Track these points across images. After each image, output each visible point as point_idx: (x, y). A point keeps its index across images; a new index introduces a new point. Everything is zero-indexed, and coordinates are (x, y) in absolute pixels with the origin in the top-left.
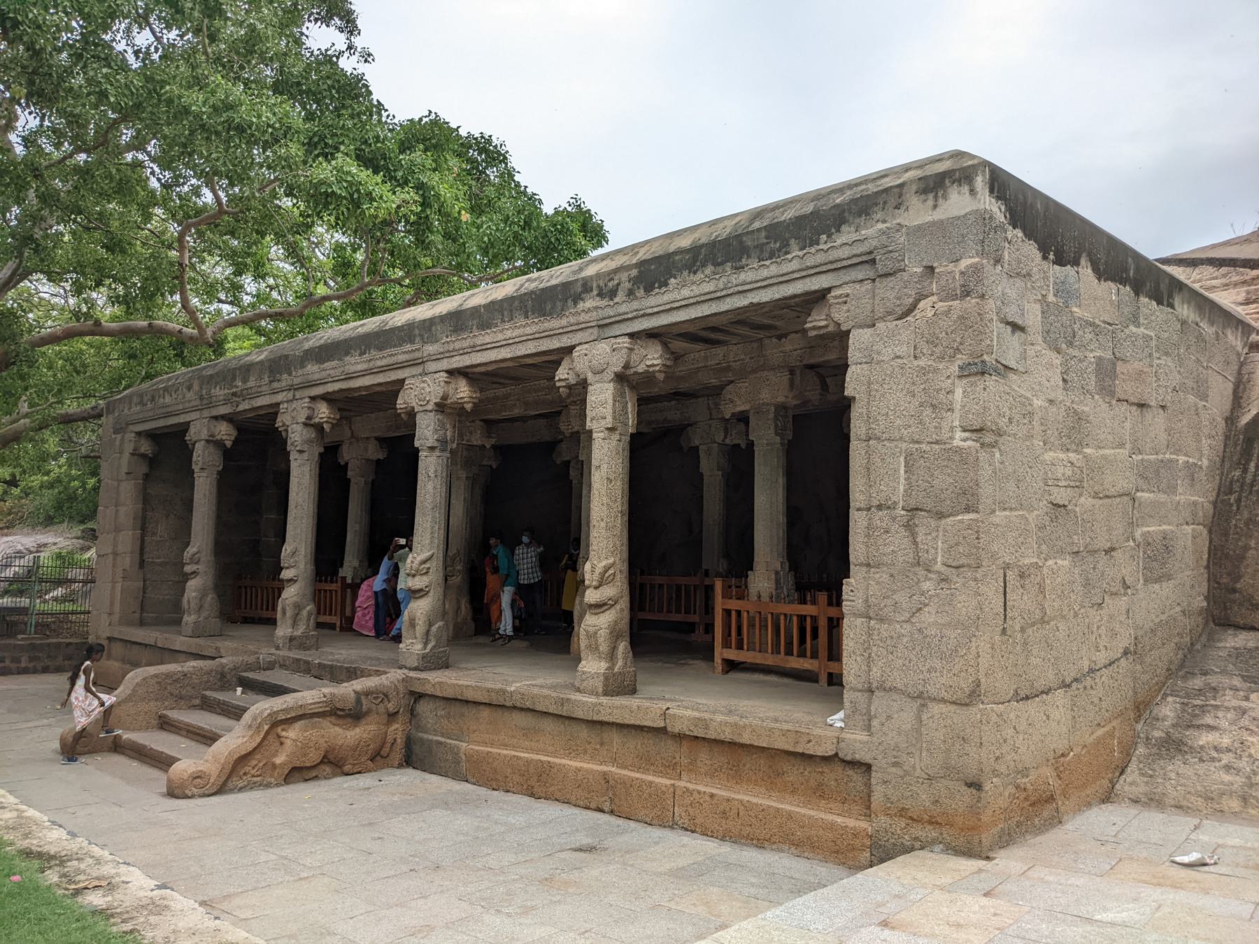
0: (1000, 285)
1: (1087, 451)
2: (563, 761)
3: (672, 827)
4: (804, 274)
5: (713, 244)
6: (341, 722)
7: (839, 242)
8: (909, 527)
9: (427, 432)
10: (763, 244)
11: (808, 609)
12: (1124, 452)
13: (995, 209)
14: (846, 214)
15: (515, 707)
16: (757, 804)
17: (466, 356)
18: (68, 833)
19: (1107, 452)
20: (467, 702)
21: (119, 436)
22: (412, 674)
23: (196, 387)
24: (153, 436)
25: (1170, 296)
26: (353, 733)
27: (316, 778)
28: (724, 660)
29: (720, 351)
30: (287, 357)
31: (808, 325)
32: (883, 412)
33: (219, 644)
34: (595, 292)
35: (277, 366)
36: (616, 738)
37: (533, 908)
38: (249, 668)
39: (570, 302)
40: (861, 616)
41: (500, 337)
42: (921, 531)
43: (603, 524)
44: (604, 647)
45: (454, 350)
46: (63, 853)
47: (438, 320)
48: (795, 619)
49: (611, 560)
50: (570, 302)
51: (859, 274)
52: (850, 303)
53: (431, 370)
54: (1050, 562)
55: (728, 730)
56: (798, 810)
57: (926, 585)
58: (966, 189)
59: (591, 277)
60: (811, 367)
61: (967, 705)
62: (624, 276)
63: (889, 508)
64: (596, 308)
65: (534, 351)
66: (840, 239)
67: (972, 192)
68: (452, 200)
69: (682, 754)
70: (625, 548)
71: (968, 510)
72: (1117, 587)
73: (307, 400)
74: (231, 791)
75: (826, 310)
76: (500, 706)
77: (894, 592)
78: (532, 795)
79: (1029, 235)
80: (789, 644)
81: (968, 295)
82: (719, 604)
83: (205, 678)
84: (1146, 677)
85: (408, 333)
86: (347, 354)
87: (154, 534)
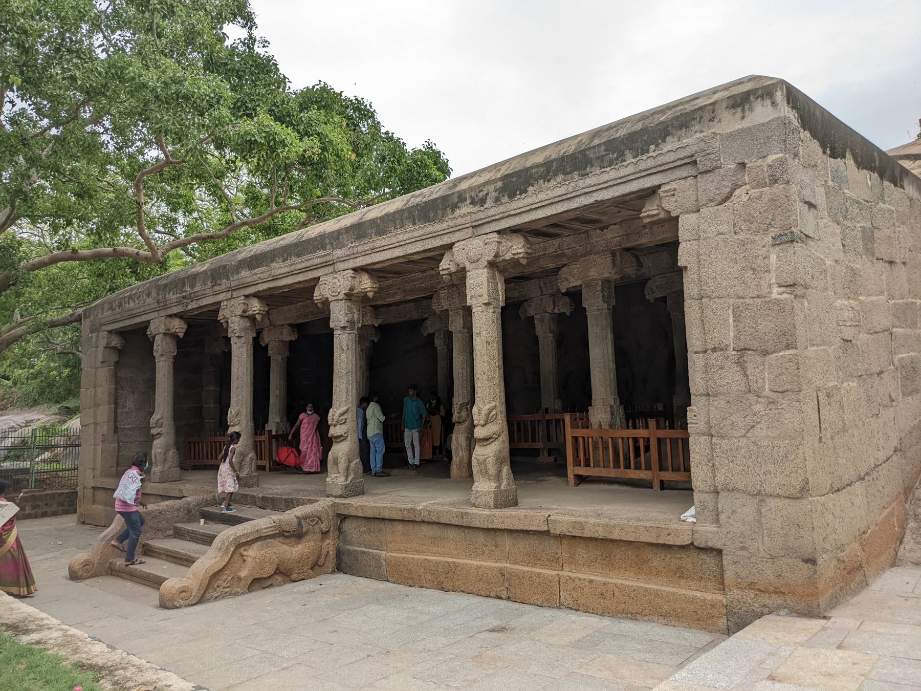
0: (798, 174)
1: (861, 298)
2: (465, 561)
3: (559, 608)
4: (638, 175)
5: (562, 159)
6: (287, 541)
7: (665, 150)
8: (740, 363)
9: (339, 315)
10: (604, 156)
11: (641, 433)
12: (883, 298)
13: (792, 117)
14: (670, 129)
15: (423, 522)
16: (629, 586)
18: (108, 646)
19: (873, 298)
20: (384, 519)
21: (95, 335)
22: (338, 501)
23: (154, 294)
24: (121, 333)
25: (902, 180)
26: (297, 549)
27: (271, 586)
28: (575, 475)
29: (556, 242)
30: (225, 267)
31: (643, 215)
32: (712, 276)
33: (181, 487)
34: (469, 201)
35: (217, 274)
36: (507, 542)
37: (475, 681)
38: (208, 503)
39: (449, 211)
40: (703, 435)
41: (394, 240)
42: (750, 366)
43: (485, 377)
44: (492, 471)
45: (358, 253)
46: (110, 664)
47: (343, 231)
48: (631, 440)
49: (493, 404)
50: (449, 211)
51: (683, 172)
52: (678, 194)
54: (845, 384)
55: (601, 530)
56: (663, 588)
57: (757, 408)
58: (768, 102)
59: (465, 190)
60: (628, 250)
61: (798, 498)
62: (491, 188)
63: (722, 350)
64: (470, 213)
65: (422, 249)
66: (666, 148)
67: (774, 104)
68: (333, 146)
69: (563, 550)
70: (503, 394)
71: (788, 347)
72: (886, 401)
73: (243, 298)
74: (208, 600)
75: (657, 202)
76: (411, 521)
77: (731, 414)
78: (442, 589)
79: (814, 135)
80: (627, 459)
81: (775, 182)
82: (569, 433)
83: (176, 514)
84: (908, 468)
85: (321, 242)
86: (272, 261)
87: (124, 407)
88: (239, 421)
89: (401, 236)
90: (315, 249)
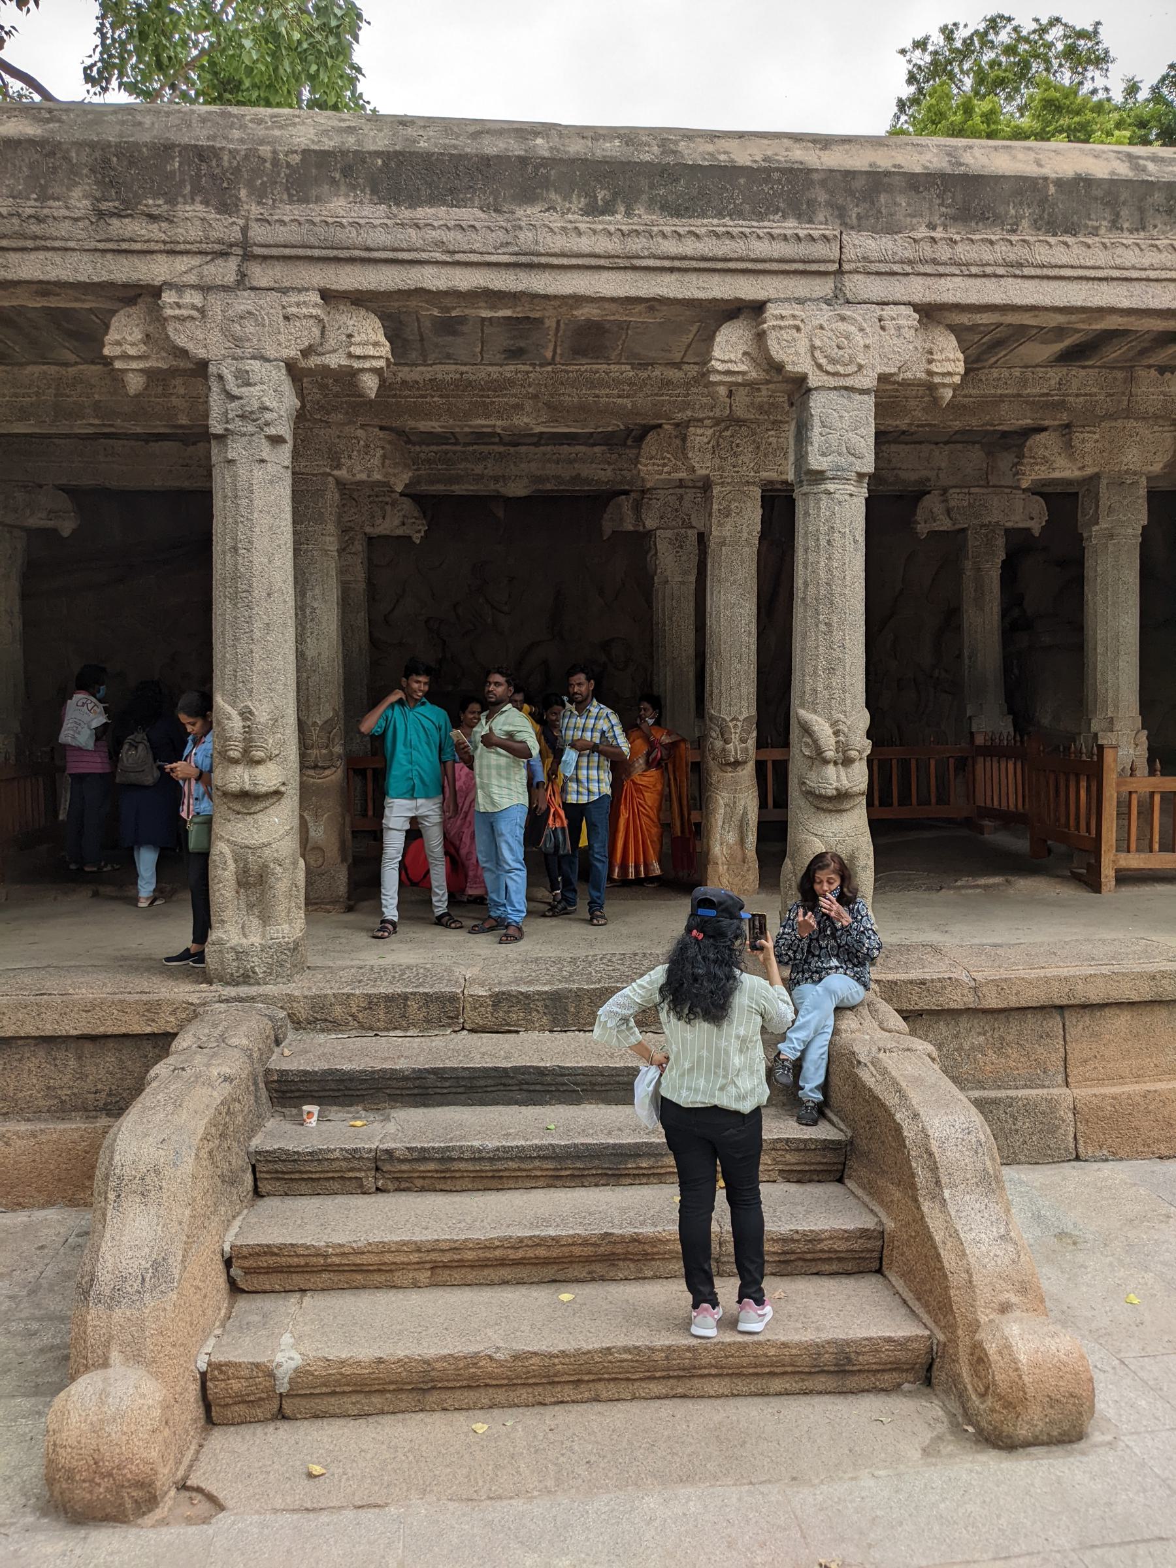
17: (990, 284)
20: (1084, 1007)
30: (202, 154)
41: (1101, 257)
73: (315, 297)
86: (527, 196)
88: (281, 744)
89: (1131, 251)
90: (761, 209)
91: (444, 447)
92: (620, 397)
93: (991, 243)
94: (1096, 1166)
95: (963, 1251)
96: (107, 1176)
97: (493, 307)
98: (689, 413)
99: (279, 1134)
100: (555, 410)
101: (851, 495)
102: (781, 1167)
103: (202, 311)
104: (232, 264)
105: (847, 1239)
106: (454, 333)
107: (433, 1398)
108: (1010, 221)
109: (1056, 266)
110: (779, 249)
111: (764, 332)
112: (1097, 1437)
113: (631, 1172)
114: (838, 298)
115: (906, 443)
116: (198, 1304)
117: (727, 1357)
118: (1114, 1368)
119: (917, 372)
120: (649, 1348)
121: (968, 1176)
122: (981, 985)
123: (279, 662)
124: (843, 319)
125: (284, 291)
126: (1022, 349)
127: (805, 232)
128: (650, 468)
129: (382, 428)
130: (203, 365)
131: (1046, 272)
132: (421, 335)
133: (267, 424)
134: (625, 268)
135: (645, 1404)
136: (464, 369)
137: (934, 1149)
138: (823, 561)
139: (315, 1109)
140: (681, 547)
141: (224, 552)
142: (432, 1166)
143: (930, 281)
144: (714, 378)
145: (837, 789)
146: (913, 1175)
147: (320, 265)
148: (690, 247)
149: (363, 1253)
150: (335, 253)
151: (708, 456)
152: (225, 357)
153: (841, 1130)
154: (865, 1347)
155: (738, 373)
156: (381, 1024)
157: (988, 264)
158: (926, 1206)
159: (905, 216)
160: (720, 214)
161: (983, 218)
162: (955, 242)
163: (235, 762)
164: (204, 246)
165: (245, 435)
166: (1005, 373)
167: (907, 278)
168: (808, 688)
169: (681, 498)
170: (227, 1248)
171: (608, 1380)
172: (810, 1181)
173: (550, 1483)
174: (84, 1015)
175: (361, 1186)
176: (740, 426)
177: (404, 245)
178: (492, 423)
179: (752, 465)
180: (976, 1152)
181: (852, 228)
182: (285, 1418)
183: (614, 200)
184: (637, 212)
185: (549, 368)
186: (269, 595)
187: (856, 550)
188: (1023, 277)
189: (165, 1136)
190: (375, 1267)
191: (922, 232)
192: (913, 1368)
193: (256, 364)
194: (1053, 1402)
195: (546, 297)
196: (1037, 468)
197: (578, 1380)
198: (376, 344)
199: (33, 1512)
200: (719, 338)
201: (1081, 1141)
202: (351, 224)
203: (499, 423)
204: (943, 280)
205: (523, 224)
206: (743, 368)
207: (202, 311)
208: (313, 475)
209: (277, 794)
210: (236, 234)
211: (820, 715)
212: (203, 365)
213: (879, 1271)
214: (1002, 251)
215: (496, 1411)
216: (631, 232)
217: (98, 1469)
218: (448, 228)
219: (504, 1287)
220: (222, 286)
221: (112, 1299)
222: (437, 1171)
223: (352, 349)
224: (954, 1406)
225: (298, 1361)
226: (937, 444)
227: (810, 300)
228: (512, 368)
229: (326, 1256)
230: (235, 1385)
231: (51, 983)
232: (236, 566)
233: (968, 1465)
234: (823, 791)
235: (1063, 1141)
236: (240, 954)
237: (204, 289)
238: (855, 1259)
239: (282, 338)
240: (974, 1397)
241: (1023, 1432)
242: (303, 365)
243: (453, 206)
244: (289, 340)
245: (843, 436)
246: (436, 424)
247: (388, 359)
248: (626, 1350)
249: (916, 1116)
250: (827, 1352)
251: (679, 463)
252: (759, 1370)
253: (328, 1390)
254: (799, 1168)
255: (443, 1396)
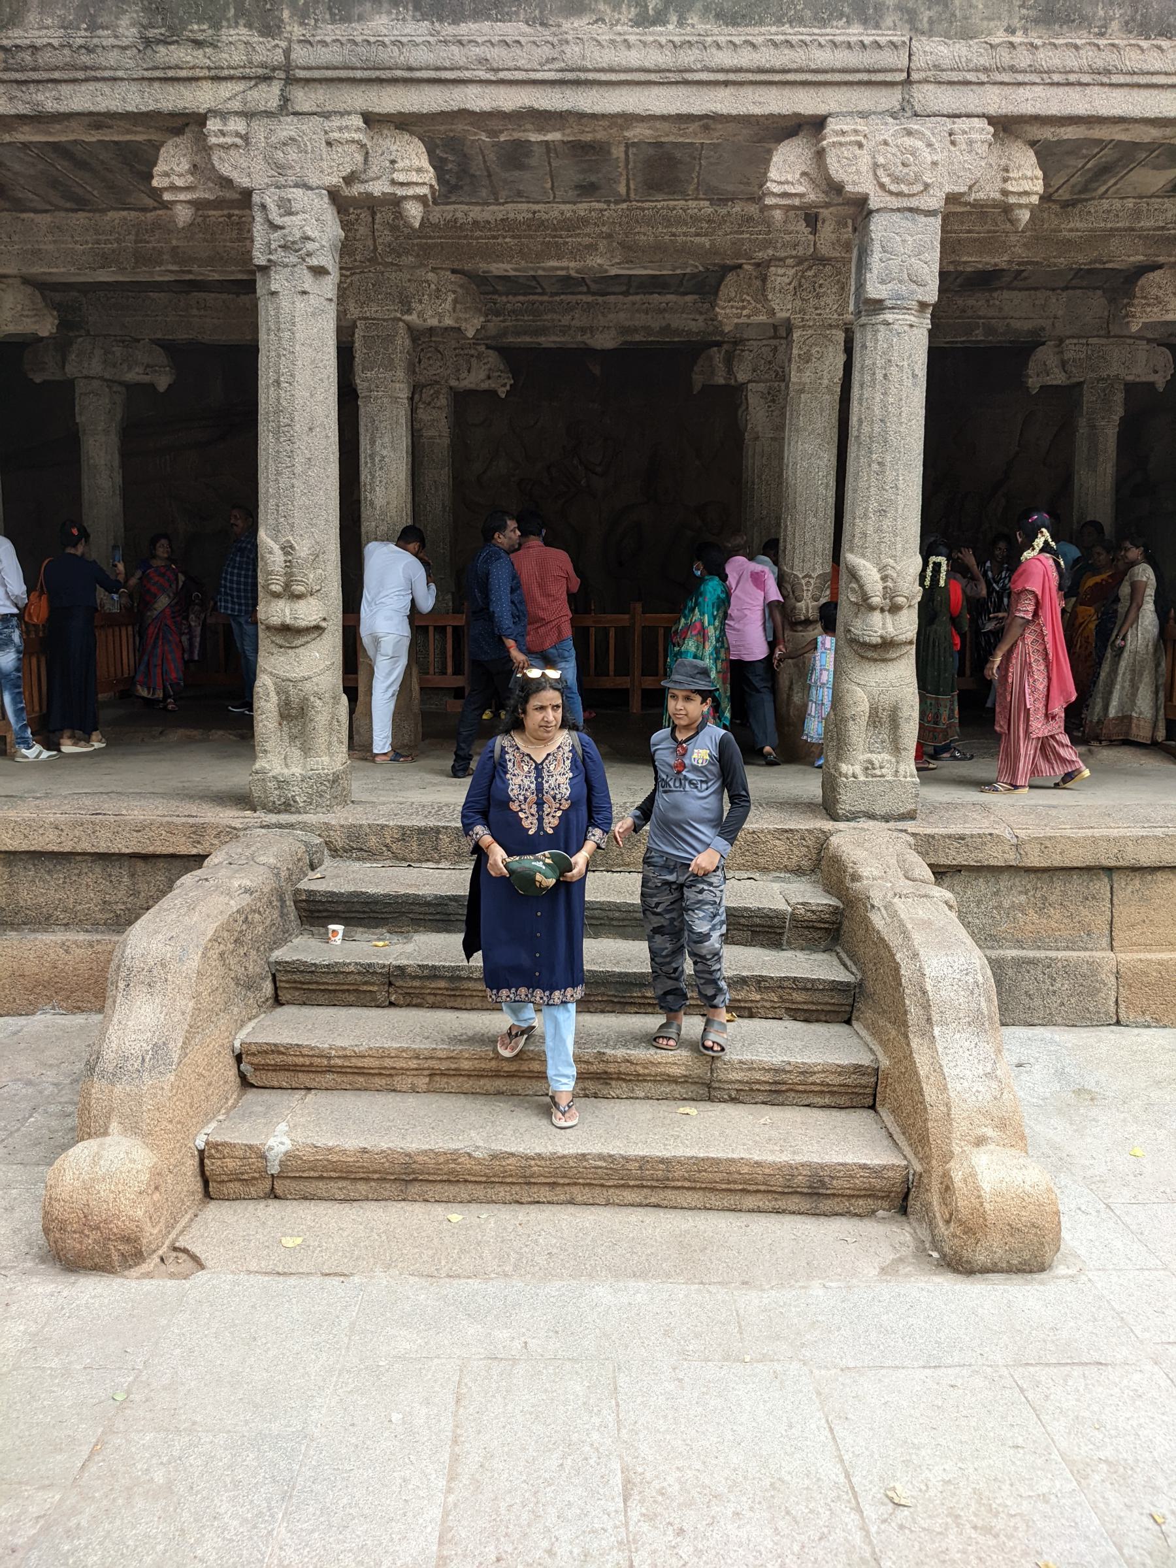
17: (1074, 94)
53: (935, 107)
73: (358, 121)
88: (322, 580)
91: (531, 297)
92: (697, 235)
93: (1076, 47)
94: (1136, 1031)
95: (945, 1085)
96: (119, 967)
97: (540, 130)
98: (770, 252)
99: (304, 949)
100: (630, 250)
101: (911, 326)
102: (787, 1005)
103: (246, 138)
104: (276, 88)
105: (840, 1074)
106: (521, 167)
107: (414, 1189)
108: (1099, 24)
109: (1148, 73)
110: (842, 58)
111: (823, 149)
112: (1061, 1270)
113: (637, 1000)
114: (907, 110)
115: (1020, 290)
116: (201, 1089)
117: (700, 1171)
118: (1098, 1211)
119: (989, 192)
120: (623, 1157)
121: (961, 1015)
122: (1024, 842)
123: (320, 498)
124: (909, 133)
125: (326, 115)
126: (1133, 177)
127: (871, 38)
128: (728, 311)
129: (454, 271)
130: (247, 194)
131: (1136, 79)
132: (488, 171)
133: (309, 254)
134: (677, 83)
135: (617, 1209)
136: (536, 207)
137: (929, 988)
138: (878, 397)
139: (340, 928)
140: (773, 401)
141: (268, 386)
142: (442, 984)
143: (1007, 90)
144: (769, 201)
145: (881, 637)
146: (906, 1013)
147: (363, 87)
148: (746, 58)
149: (364, 1057)
150: (378, 73)
151: (789, 297)
152: (268, 186)
153: (852, 973)
154: (839, 1171)
155: (795, 195)
156: (414, 856)
157: (1071, 72)
158: (915, 1042)
159: (982, 20)
160: (779, 21)
161: (1067, 21)
162: (1036, 48)
163: (277, 596)
164: (248, 70)
165: (286, 266)
166: (1117, 204)
167: (983, 88)
168: (858, 530)
169: (775, 350)
170: (237, 1044)
171: (583, 1185)
172: (817, 1021)
173: (508, 1268)
174: (135, 834)
175: (375, 1000)
176: (824, 266)
177: (447, 64)
178: (565, 263)
179: (835, 307)
180: (972, 993)
181: (923, 33)
182: (276, 1197)
183: (666, 8)
184: (690, 21)
185: (624, 206)
186: (310, 429)
187: (915, 385)
188: (1111, 85)
189: (173, 934)
190: (376, 1071)
191: (999, 37)
192: (888, 1196)
193: (298, 193)
194: (1013, 1230)
195: (594, 116)
196: (1149, 309)
197: (554, 1183)
198: (419, 170)
199: (33, 1260)
200: (777, 158)
201: (1122, 1006)
202: (393, 43)
203: (572, 264)
204: (1021, 90)
205: (570, 37)
206: (801, 189)
207: (246, 138)
208: (384, 320)
209: (318, 629)
210: (278, 57)
211: (868, 560)
212: (247, 194)
213: (873, 1107)
214: (1089, 56)
215: (473, 1206)
216: (683, 43)
217: (87, 1223)
218: (492, 44)
219: (498, 1097)
220: (266, 112)
221: (114, 1075)
222: (447, 989)
223: (395, 176)
224: (924, 1233)
225: (288, 1145)
226: (1053, 290)
227: (874, 113)
228: (585, 206)
229: (330, 1058)
230: (231, 1164)
231: (109, 806)
232: (278, 400)
233: (922, 1285)
234: (867, 639)
235: (1103, 1004)
236: (282, 783)
237: (248, 115)
238: (847, 1093)
239: (324, 165)
240: (941, 1224)
241: (981, 1258)
242: (347, 193)
243: (498, 20)
244: (331, 167)
245: (906, 263)
246: (508, 267)
247: (431, 186)
248: (601, 1157)
249: (916, 955)
250: (800, 1174)
251: (759, 306)
252: (732, 1186)
253: (316, 1174)
254: (806, 1007)
255: (424, 1188)
